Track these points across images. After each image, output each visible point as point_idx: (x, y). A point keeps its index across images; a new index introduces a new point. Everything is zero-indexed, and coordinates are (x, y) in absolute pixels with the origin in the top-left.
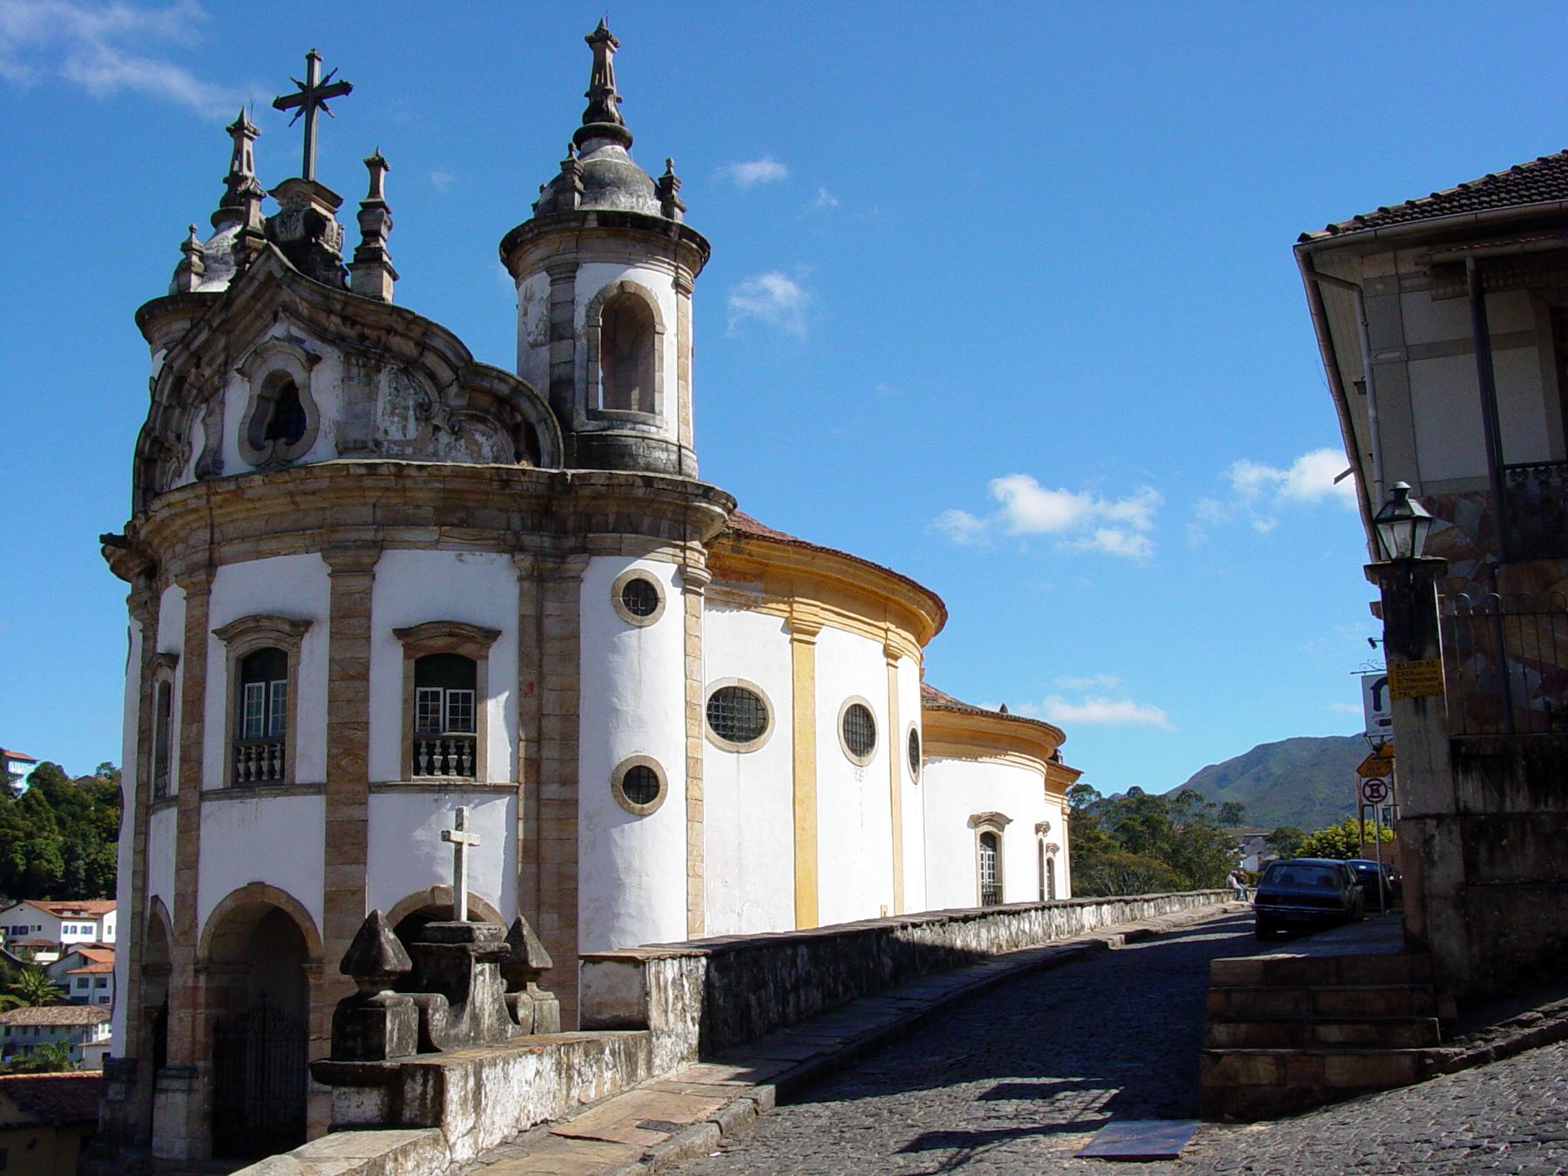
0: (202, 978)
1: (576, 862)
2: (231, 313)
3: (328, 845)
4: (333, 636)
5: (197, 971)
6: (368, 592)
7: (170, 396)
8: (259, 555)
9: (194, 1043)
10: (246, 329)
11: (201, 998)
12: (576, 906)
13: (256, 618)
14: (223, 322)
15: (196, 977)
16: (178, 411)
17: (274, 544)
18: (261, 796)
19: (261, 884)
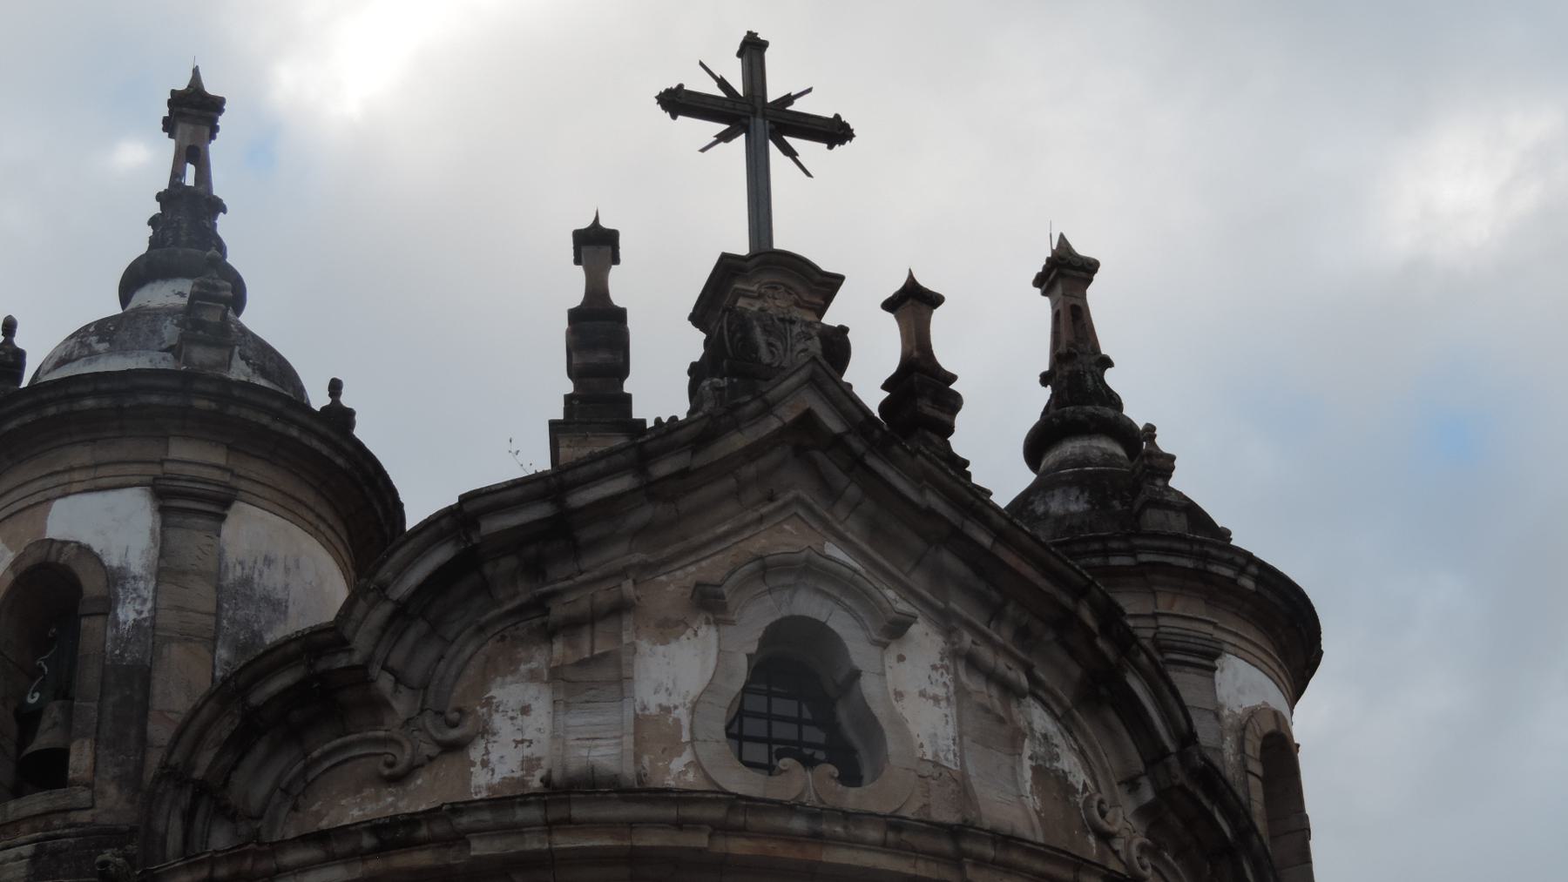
2: (702, 460)
14: (683, 473)
16: (419, 627)
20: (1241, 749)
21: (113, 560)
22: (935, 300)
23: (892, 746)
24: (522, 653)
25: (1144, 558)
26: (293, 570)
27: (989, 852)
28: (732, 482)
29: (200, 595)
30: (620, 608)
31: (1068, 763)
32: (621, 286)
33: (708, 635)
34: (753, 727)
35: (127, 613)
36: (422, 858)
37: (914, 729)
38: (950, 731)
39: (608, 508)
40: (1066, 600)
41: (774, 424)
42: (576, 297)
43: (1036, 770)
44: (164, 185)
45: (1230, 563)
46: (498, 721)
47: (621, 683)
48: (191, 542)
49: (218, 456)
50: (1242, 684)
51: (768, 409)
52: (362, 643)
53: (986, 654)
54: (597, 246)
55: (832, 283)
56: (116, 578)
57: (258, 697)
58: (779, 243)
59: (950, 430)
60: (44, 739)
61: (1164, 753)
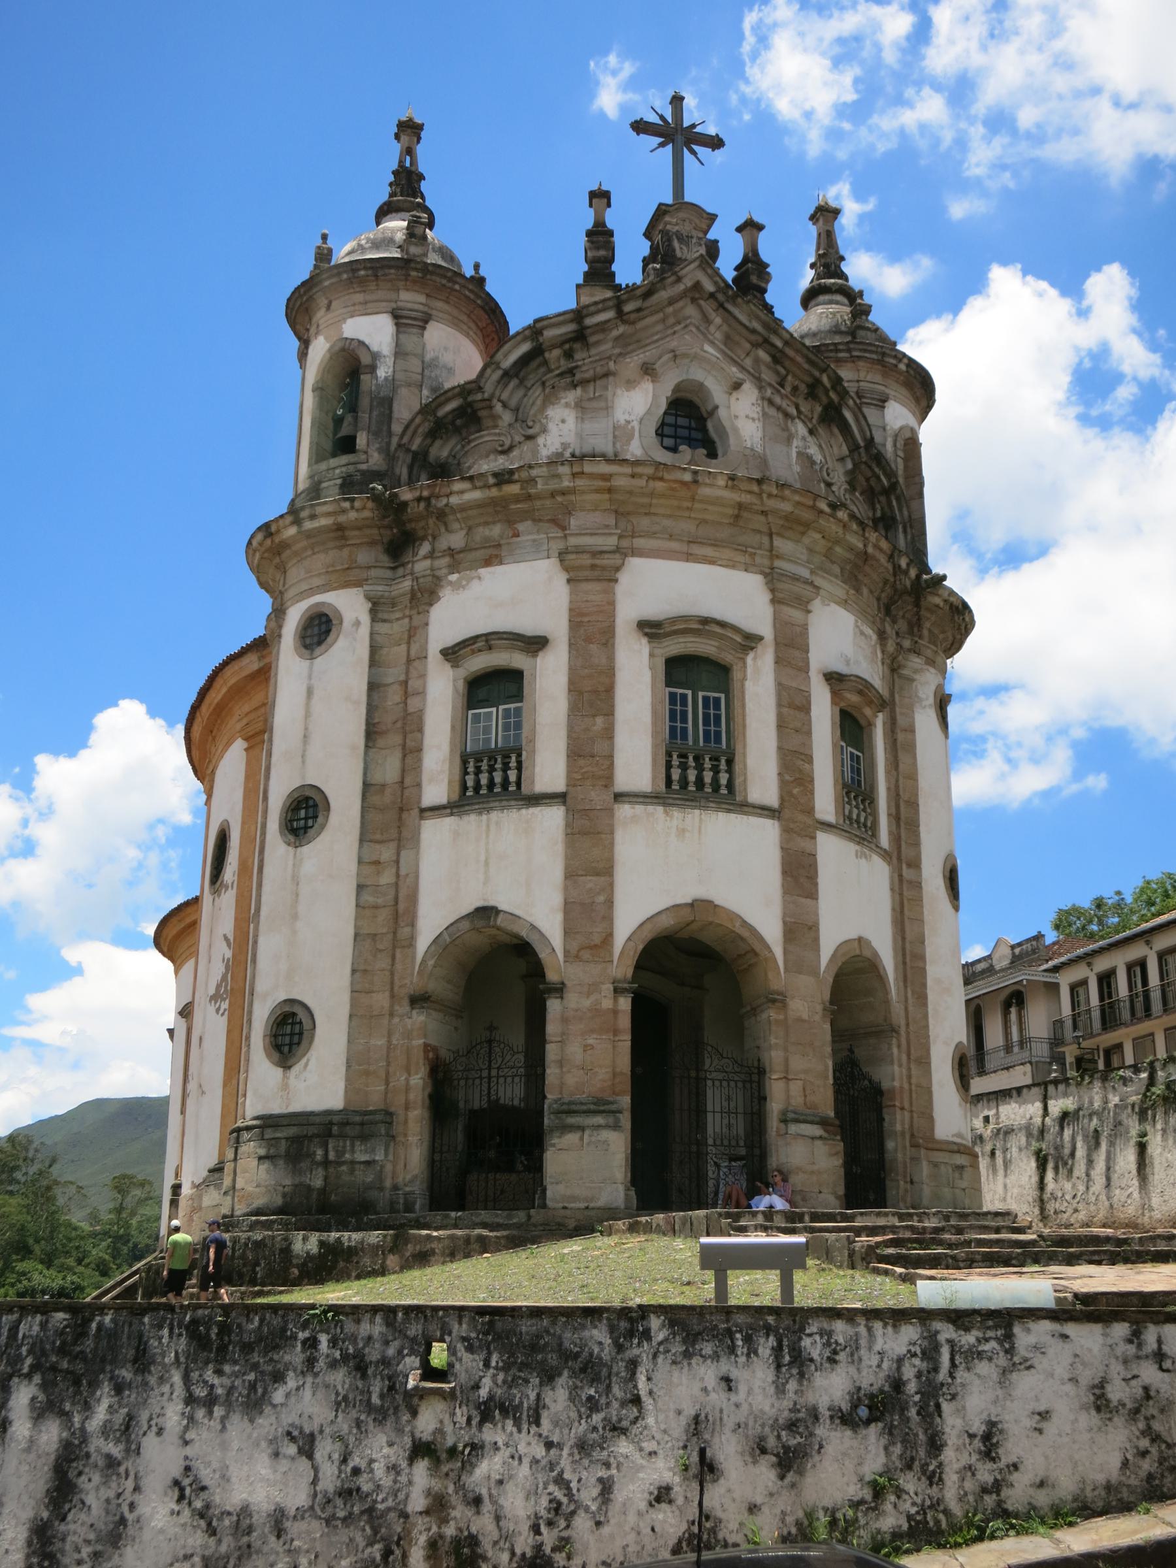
0: (625, 1003)
1: (923, 942)
2: (647, 304)
3: (785, 873)
4: (778, 661)
5: (616, 990)
6: (805, 627)
7: (515, 363)
8: (689, 557)
9: (614, 1075)
10: (647, 327)
11: (625, 1022)
12: (924, 985)
13: (706, 621)
14: (639, 310)
15: (615, 999)
16: (514, 382)
17: (709, 551)
18: (706, 808)
19: (711, 902)
20: (895, 445)
21: (375, 348)
22: (760, 228)
23: (732, 441)
24: (562, 394)
25: (855, 353)
26: (456, 354)
27: (775, 492)
28: (661, 315)
29: (415, 365)
30: (606, 375)
31: (814, 451)
32: (612, 219)
33: (647, 386)
34: (667, 430)
35: (382, 372)
36: (514, 489)
37: (742, 433)
38: (760, 434)
39: (602, 327)
40: (817, 374)
41: (681, 287)
42: (590, 225)
43: (799, 453)
44: (395, 166)
45: (895, 357)
46: (551, 426)
47: (608, 409)
48: (410, 341)
49: (422, 298)
50: (897, 414)
51: (679, 280)
52: (489, 388)
53: (778, 400)
54: (600, 197)
55: (712, 218)
56: (375, 356)
57: (441, 413)
58: (688, 198)
59: (765, 291)
60: (345, 431)
61: (858, 447)
